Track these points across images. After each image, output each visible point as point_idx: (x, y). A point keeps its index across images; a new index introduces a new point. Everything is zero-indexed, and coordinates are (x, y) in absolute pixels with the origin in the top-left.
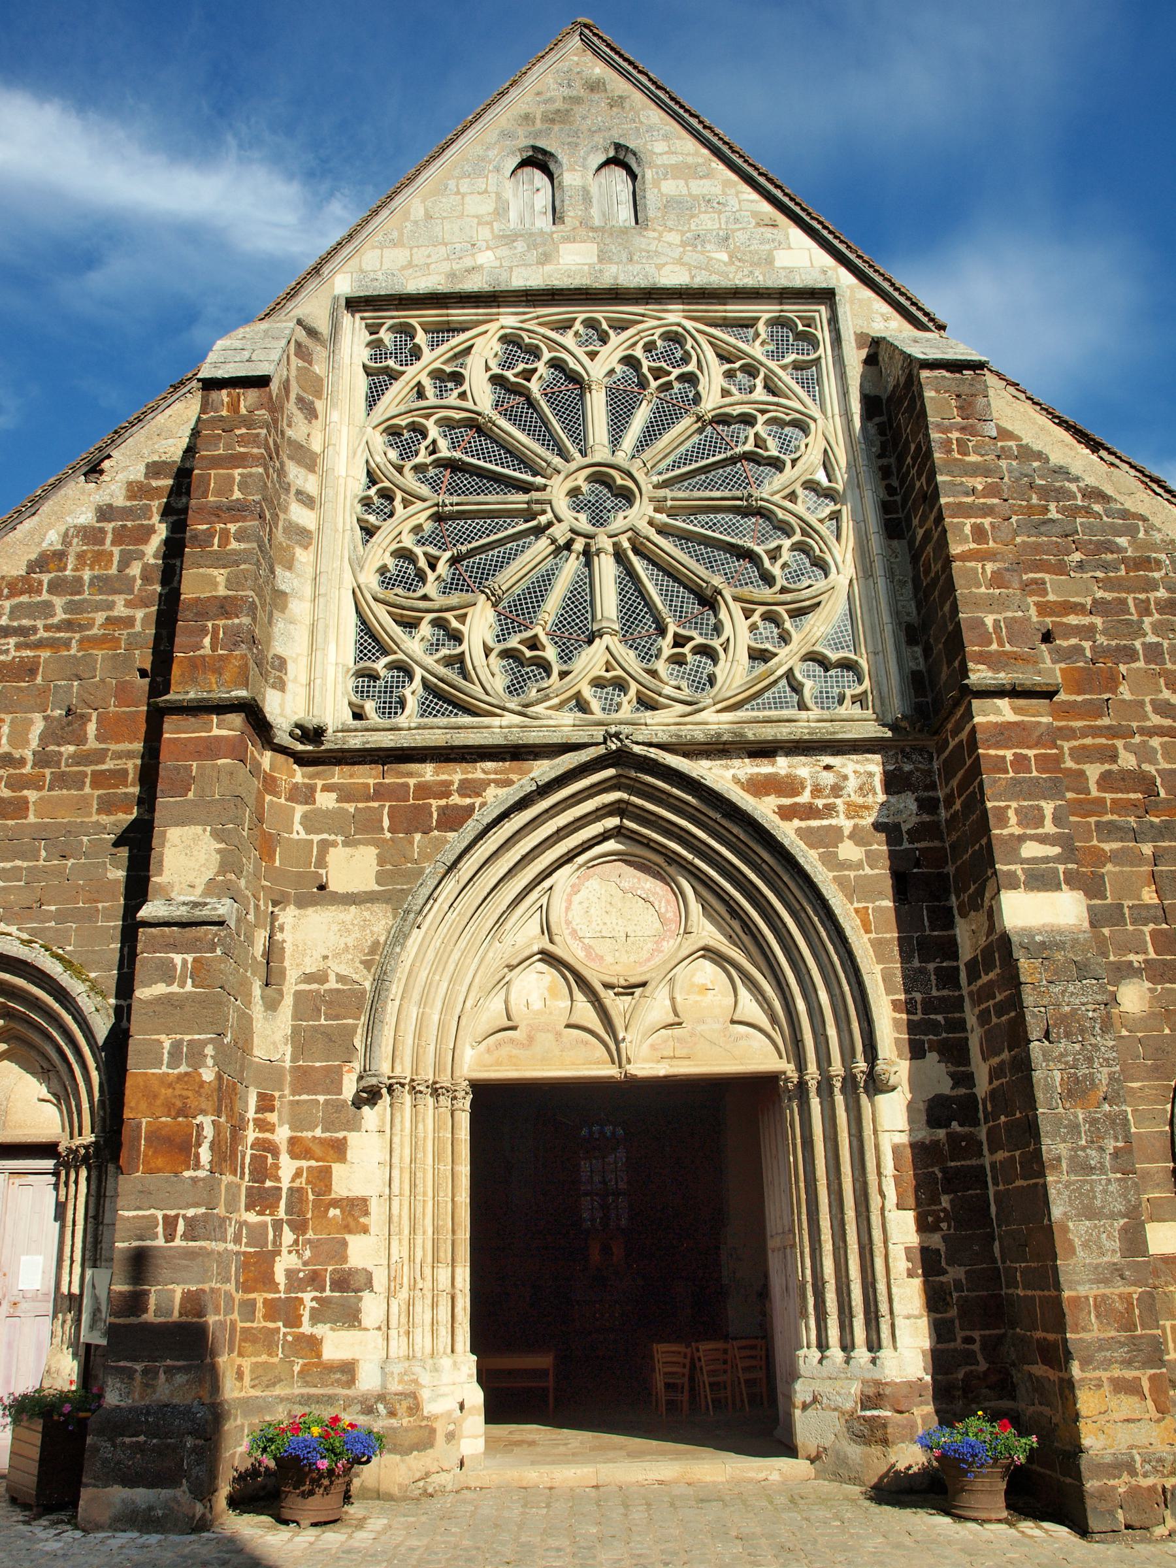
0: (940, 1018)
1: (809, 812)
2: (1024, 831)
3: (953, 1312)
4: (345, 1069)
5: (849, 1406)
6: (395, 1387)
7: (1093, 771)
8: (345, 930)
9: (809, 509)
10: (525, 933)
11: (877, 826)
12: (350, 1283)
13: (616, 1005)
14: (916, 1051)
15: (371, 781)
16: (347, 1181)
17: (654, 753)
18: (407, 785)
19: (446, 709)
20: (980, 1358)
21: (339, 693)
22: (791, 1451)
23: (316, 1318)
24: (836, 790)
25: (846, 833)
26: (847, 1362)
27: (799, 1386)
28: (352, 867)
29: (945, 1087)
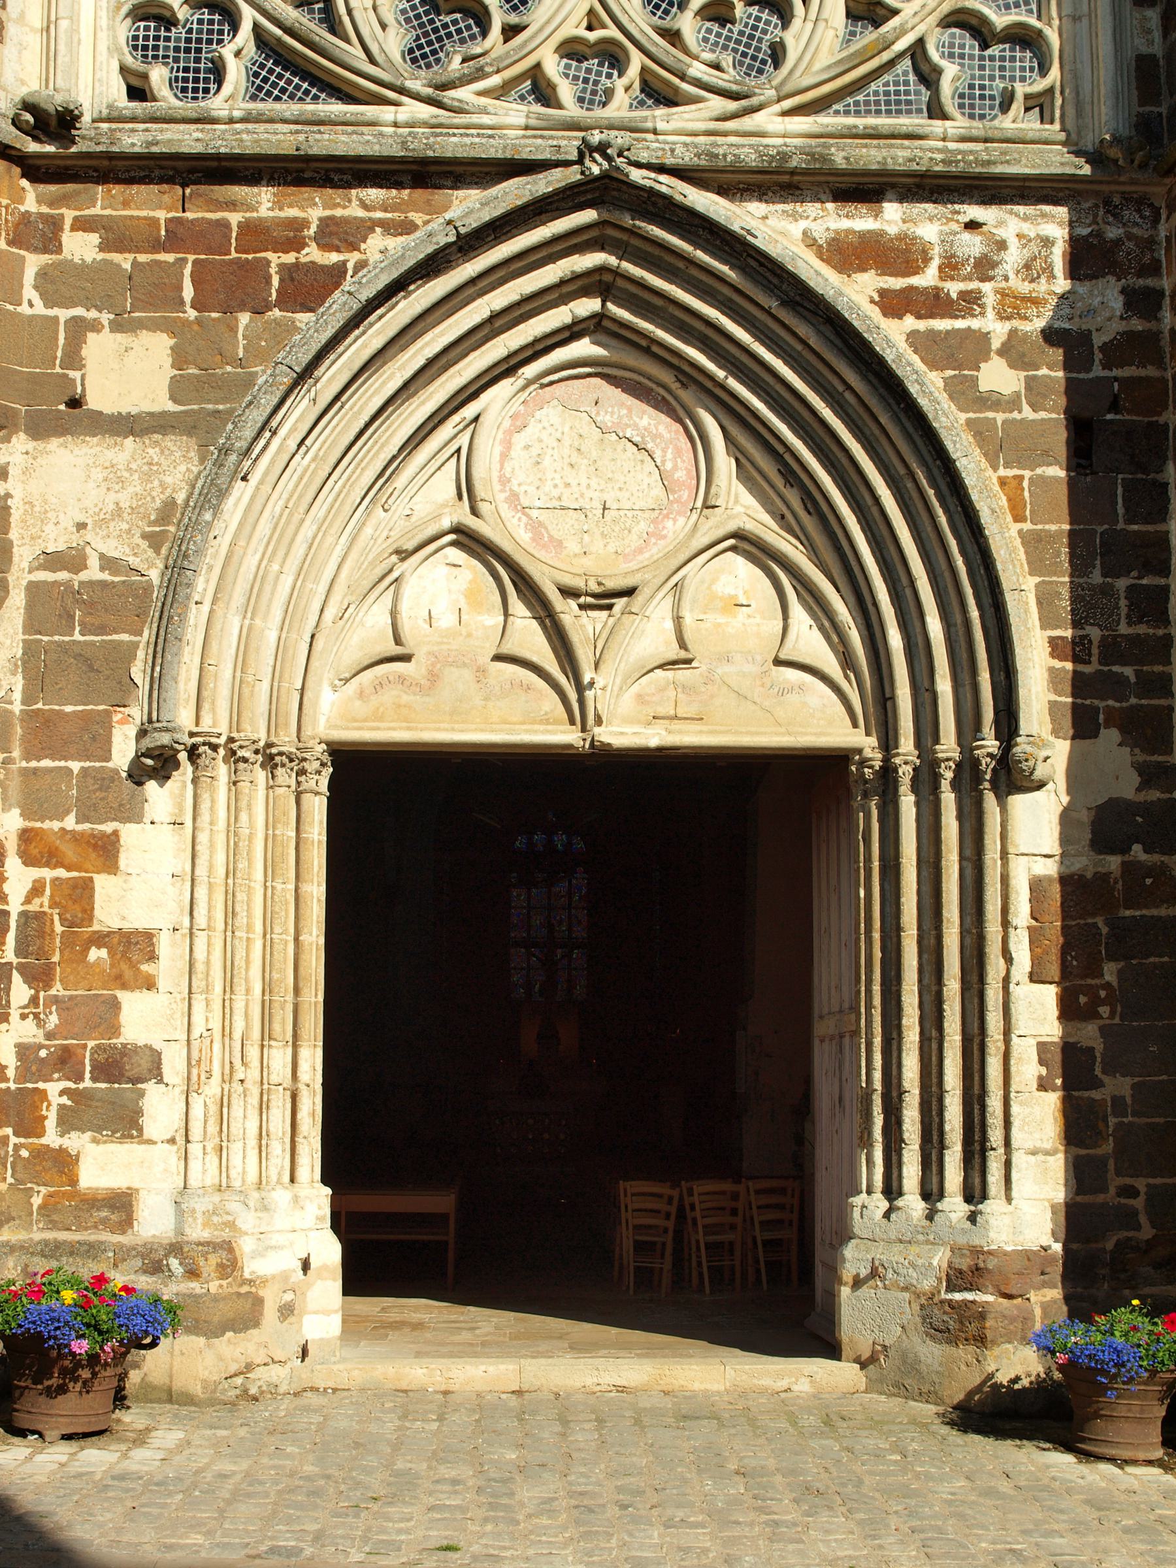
0: (1128, 671)
1: (934, 303)
3: (1108, 1147)
4: (116, 718)
5: (927, 1284)
6: (197, 1232)
8: (115, 478)
10: (430, 497)
11: (1050, 335)
12: (126, 1069)
13: (585, 627)
14: (1083, 725)
15: (162, 215)
16: (117, 903)
17: (666, 184)
18: (226, 225)
19: (298, 88)
20: (1143, 1219)
21: (102, 47)
22: (831, 1349)
23: (67, 1122)
24: (985, 267)
25: (996, 344)
26: (930, 1216)
27: (849, 1251)
28: (129, 369)
29: (1127, 787)
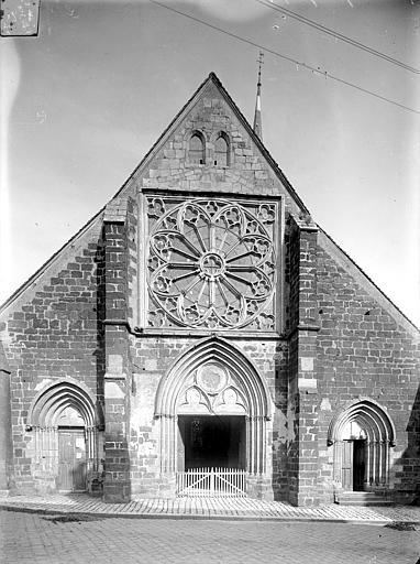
2: (306, 364)
7: (326, 348)
9: (267, 270)
10: (191, 382)
28: (151, 365)
